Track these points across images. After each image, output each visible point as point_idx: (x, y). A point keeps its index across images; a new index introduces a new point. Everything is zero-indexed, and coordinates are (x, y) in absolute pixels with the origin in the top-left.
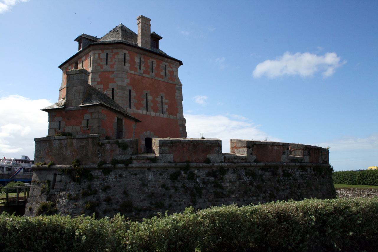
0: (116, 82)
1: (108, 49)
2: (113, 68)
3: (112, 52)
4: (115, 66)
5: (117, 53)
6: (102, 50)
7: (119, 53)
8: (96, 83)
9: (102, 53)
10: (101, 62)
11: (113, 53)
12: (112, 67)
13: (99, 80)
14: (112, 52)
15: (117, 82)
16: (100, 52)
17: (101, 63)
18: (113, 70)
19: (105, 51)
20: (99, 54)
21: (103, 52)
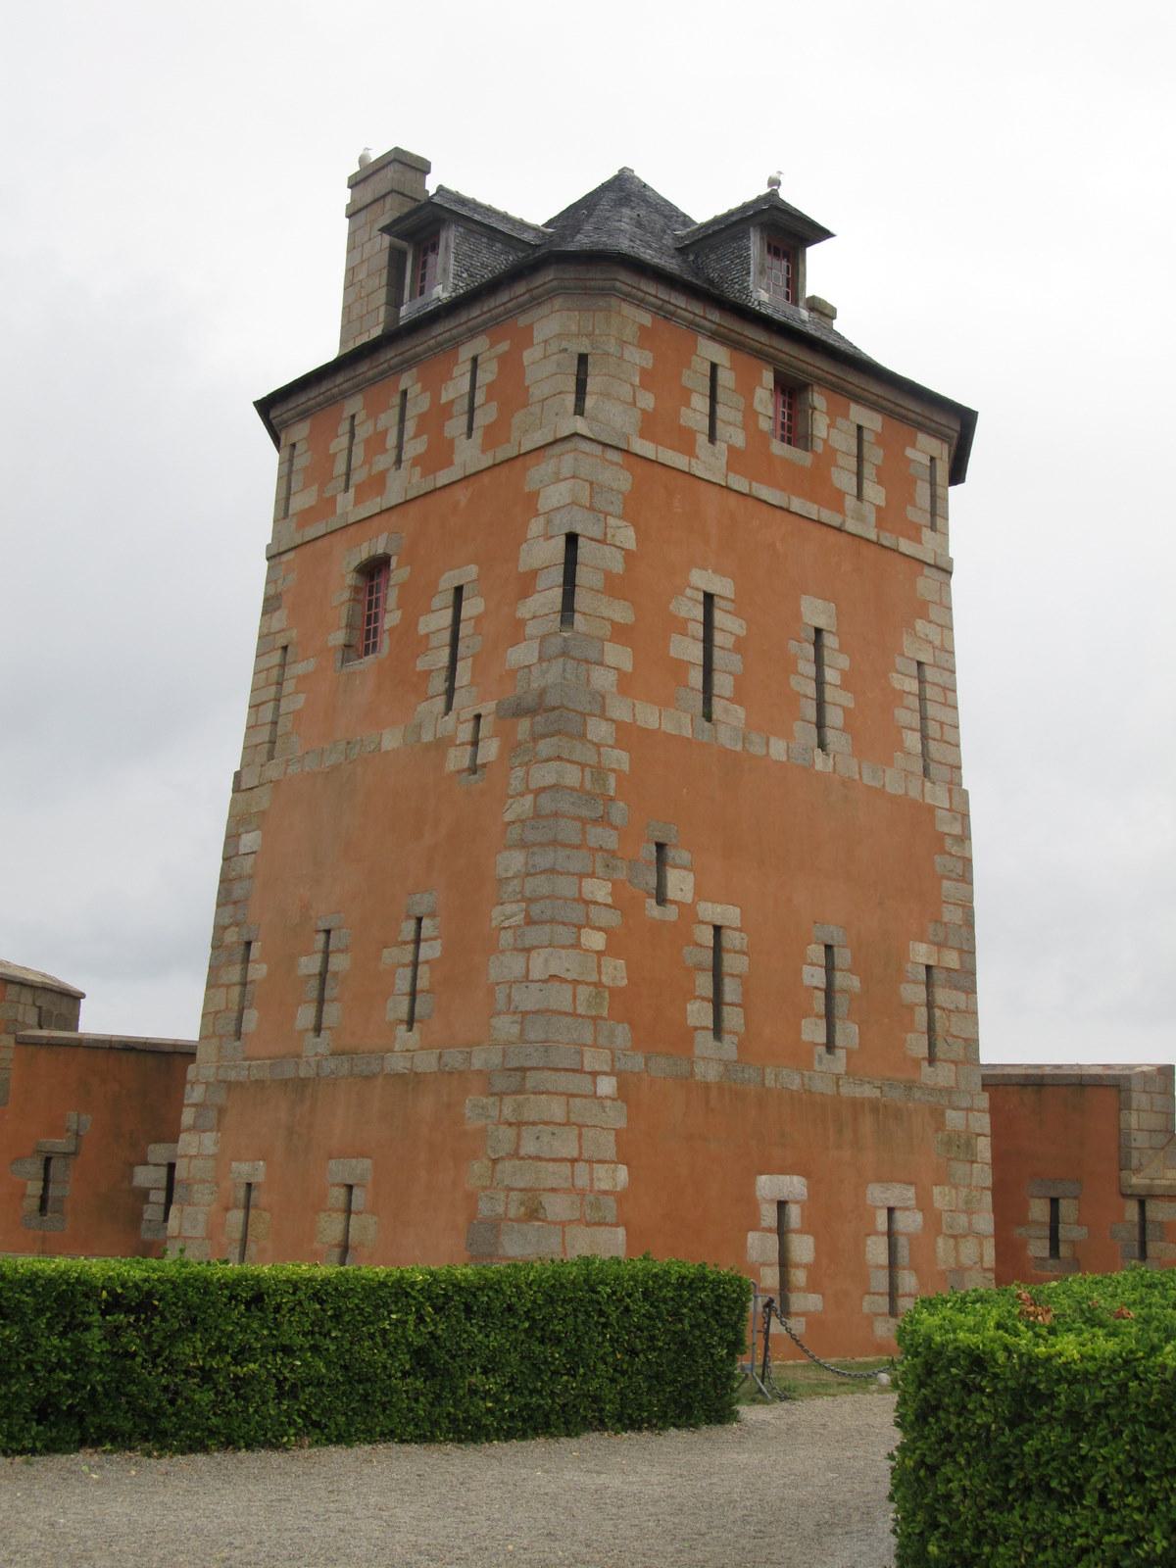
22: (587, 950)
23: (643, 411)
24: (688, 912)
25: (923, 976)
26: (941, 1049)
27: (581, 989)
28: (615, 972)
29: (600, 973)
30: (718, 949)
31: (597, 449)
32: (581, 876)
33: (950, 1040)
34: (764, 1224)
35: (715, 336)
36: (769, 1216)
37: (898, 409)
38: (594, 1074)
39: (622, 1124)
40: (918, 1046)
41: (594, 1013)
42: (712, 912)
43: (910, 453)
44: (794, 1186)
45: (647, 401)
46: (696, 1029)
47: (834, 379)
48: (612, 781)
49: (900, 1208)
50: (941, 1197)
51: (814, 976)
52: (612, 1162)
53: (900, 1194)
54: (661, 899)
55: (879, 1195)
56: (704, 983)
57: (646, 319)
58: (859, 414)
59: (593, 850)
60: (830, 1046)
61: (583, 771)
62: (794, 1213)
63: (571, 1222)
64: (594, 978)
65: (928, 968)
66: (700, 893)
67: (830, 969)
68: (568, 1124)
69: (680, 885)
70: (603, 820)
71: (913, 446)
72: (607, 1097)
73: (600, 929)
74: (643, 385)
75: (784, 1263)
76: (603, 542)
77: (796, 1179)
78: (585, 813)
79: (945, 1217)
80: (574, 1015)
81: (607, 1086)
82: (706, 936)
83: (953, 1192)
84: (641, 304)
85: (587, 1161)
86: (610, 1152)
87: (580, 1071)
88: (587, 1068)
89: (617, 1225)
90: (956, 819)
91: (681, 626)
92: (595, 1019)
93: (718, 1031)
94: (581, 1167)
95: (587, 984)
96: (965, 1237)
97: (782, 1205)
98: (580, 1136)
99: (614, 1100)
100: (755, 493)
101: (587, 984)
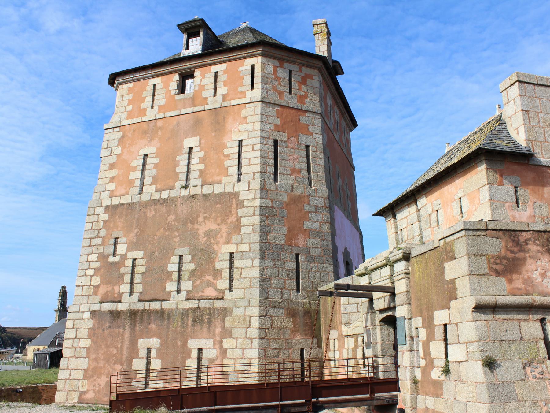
0: (312, 134)
1: (294, 63)
2: (305, 104)
3: (300, 71)
4: (307, 102)
5: (311, 77)
6: (281, 61)
7: (314, 77)
8: (272, 126)
9: (280, 67)
10: (280, 84)
11: (303, 75)
12: (302, 99)
13: (278, 121)
14: (300, 71)
15: (314, 135)
16: (277, 63)
17: (279, 88)
18: (305, 107)
19: (286, 65)
20: (275, 67)
21: (281, 66)
22: (88, 276)
23: (129, 112)
24: (124, 257)
25: (228, 257)
26: (235, 284)
27: (84, 287)
28: (96, 280)
29: (91, 281)
30: (133, 266)
31: (112, 129)
32: (88, 255)
33: (241, 280)
34: (140, 356)
35: (153, 77)
36: (143, 353)
37: (230, 58)
38: (83, 312)
39: (91, 326)
40: (223, 284)
41: (88, 294)
42: (132, 254)
43: (240, 69)
44: (155, 342)
45: (130, 108)
46: (123, 293)
47: (200, 64)
48: (102, 223)
49: (205, 349)
50: (227, 343)
51: (173, 267)
52: (86, 338)
53: (205, 343)
54: (114, 255)
55: (193, 344)
56: (128, 278)
57: (131, 85)
58: (214, 68)
59: (93, 246)
60: (179, 291)
61: (92, 224)
62: (154, 353)
63: (71, 357)
64: (89, 284)
65: (232, 254)
66: (128, 250)
67: (180, 263)
68: (73, 328)
69: (121, 249)
70: (98, 236)
71: (243, 65)
72: (86, 319)
73: (92, 269)
74: (129, 104)
75: (148, 370)
76: (111, 155)
77: (155, 340)
78: (92, 236)
79: (228, 351)
80: (82, 295)
81: (87, 315)
82: (129, 263)
83: (234, 341)
84: (127, 82)
85: (78, 339)
86: (86, 335)
87: (79, 312)
88: (80, 311)
89: (85, 358)
90: (251, 192)
91: (134, 169)
92: (88, 295)
93: (131, 294)
94: (76, 340)
95: (87, 286)
96: (240, 359)
97: (149, 349)
98: (77, 331)
99: (89, 319)
100: (166, 116)
101: (87, 286)
